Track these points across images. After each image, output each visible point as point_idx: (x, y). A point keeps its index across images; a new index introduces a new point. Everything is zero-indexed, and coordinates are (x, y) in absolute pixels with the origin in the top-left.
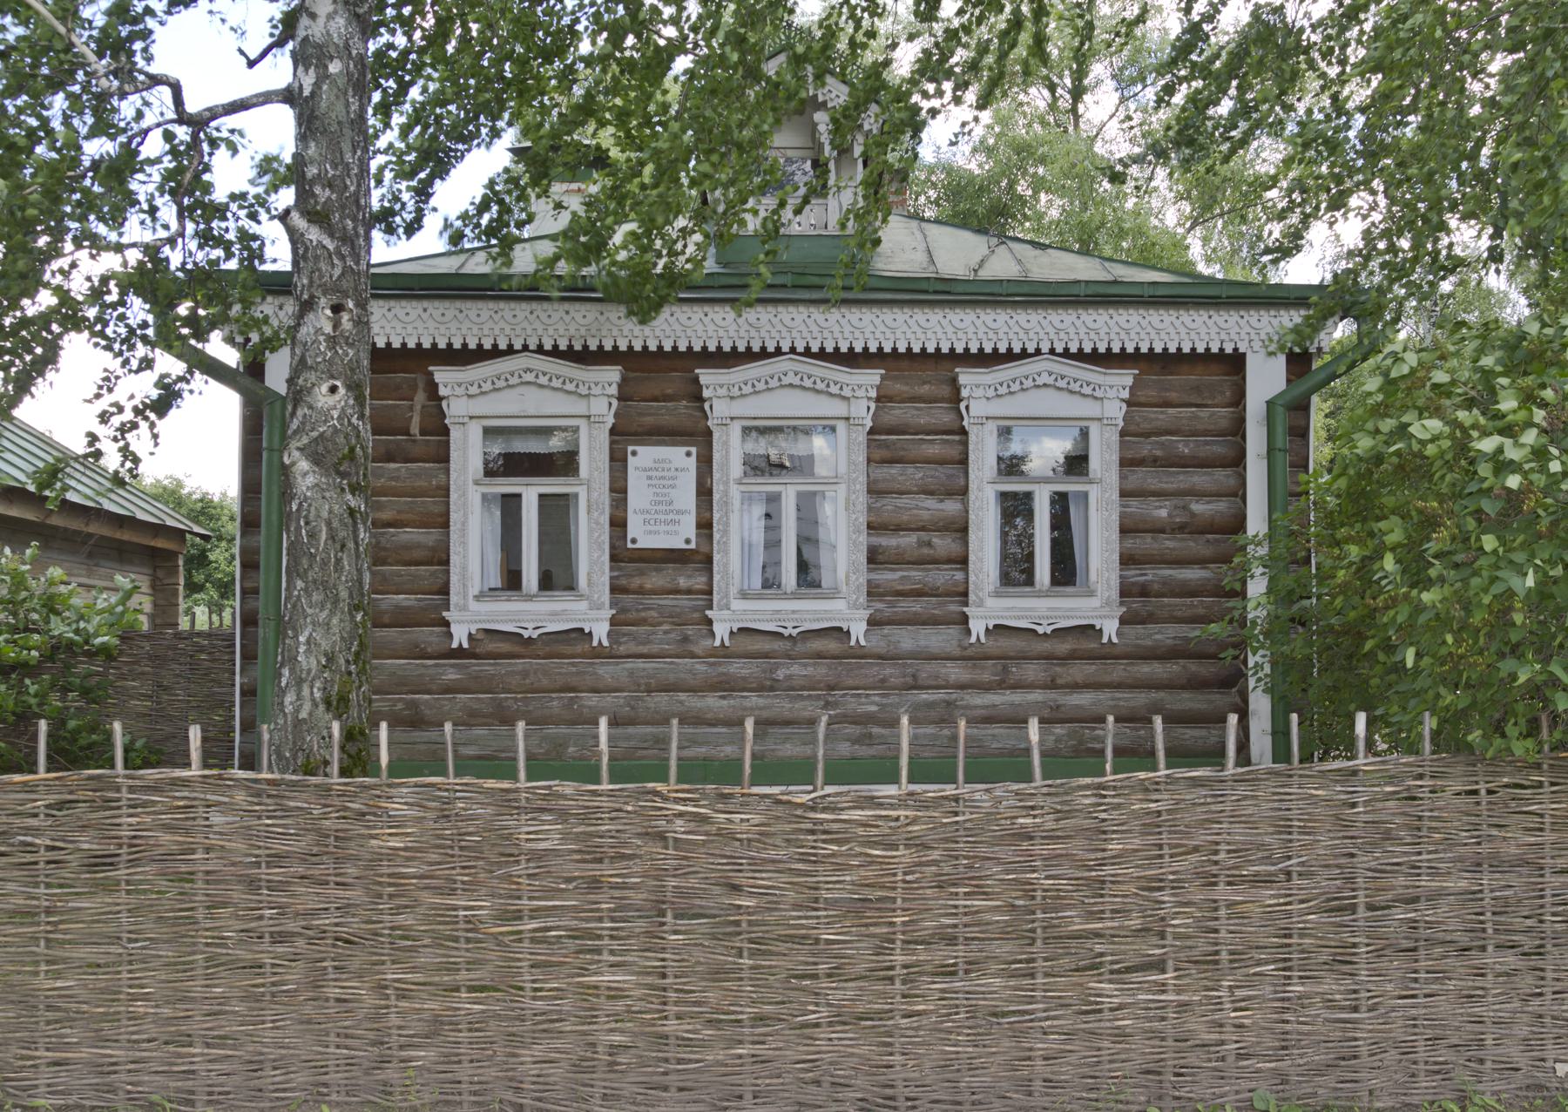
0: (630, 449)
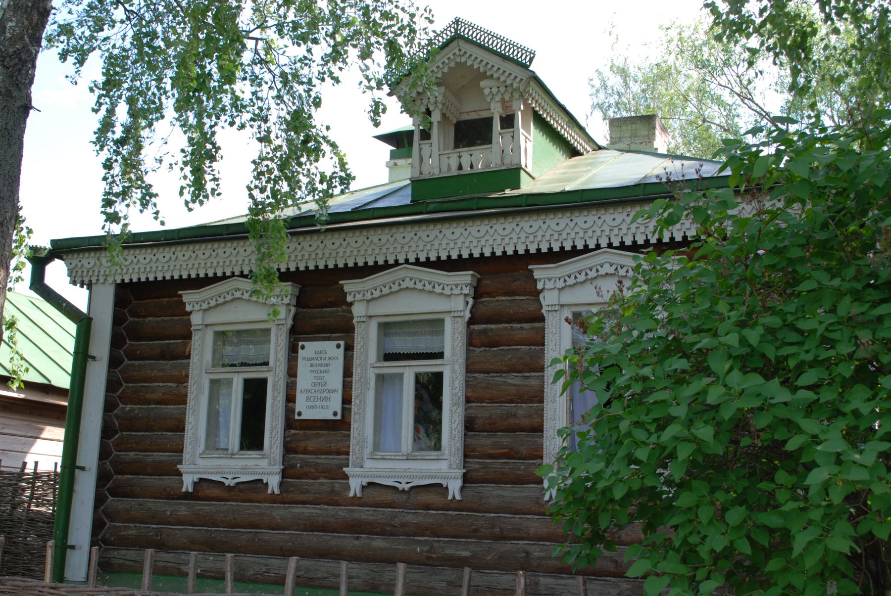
0: (300, 344)
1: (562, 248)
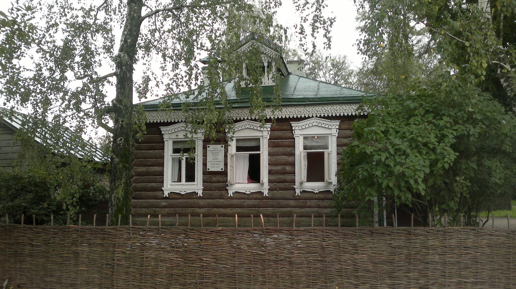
0: (208, 146)
1: (301, 117)
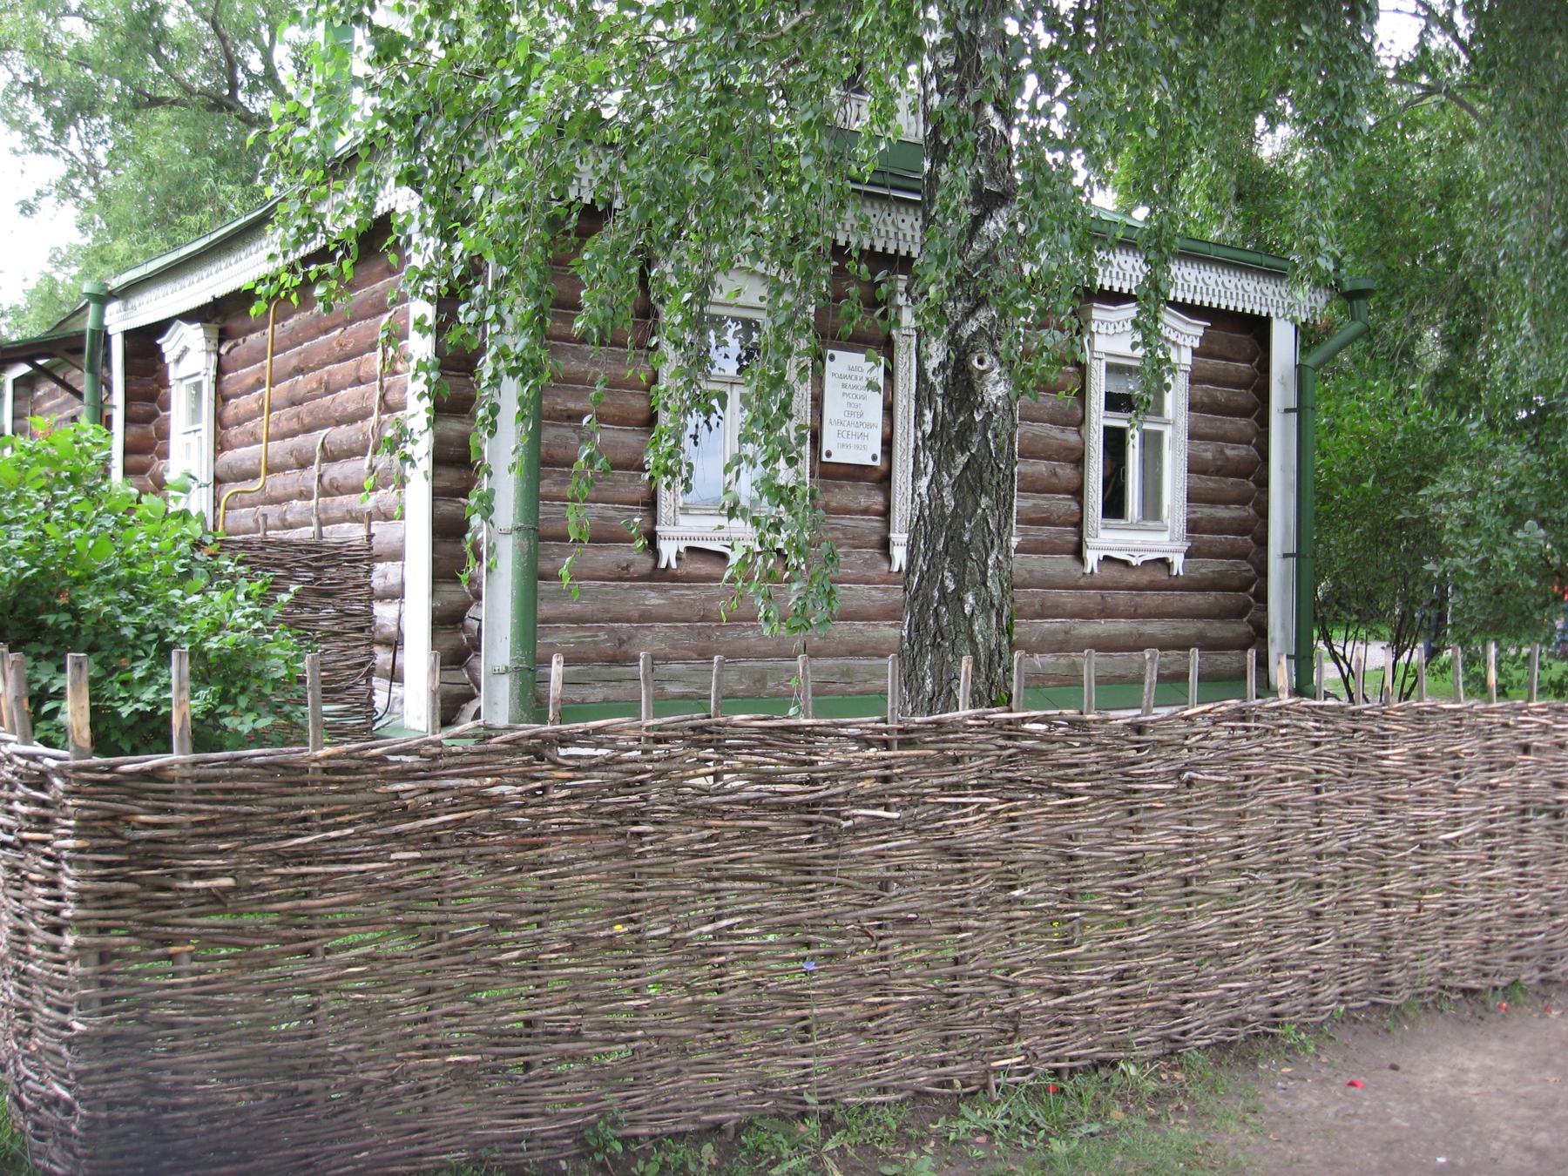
0: (830, 352)
